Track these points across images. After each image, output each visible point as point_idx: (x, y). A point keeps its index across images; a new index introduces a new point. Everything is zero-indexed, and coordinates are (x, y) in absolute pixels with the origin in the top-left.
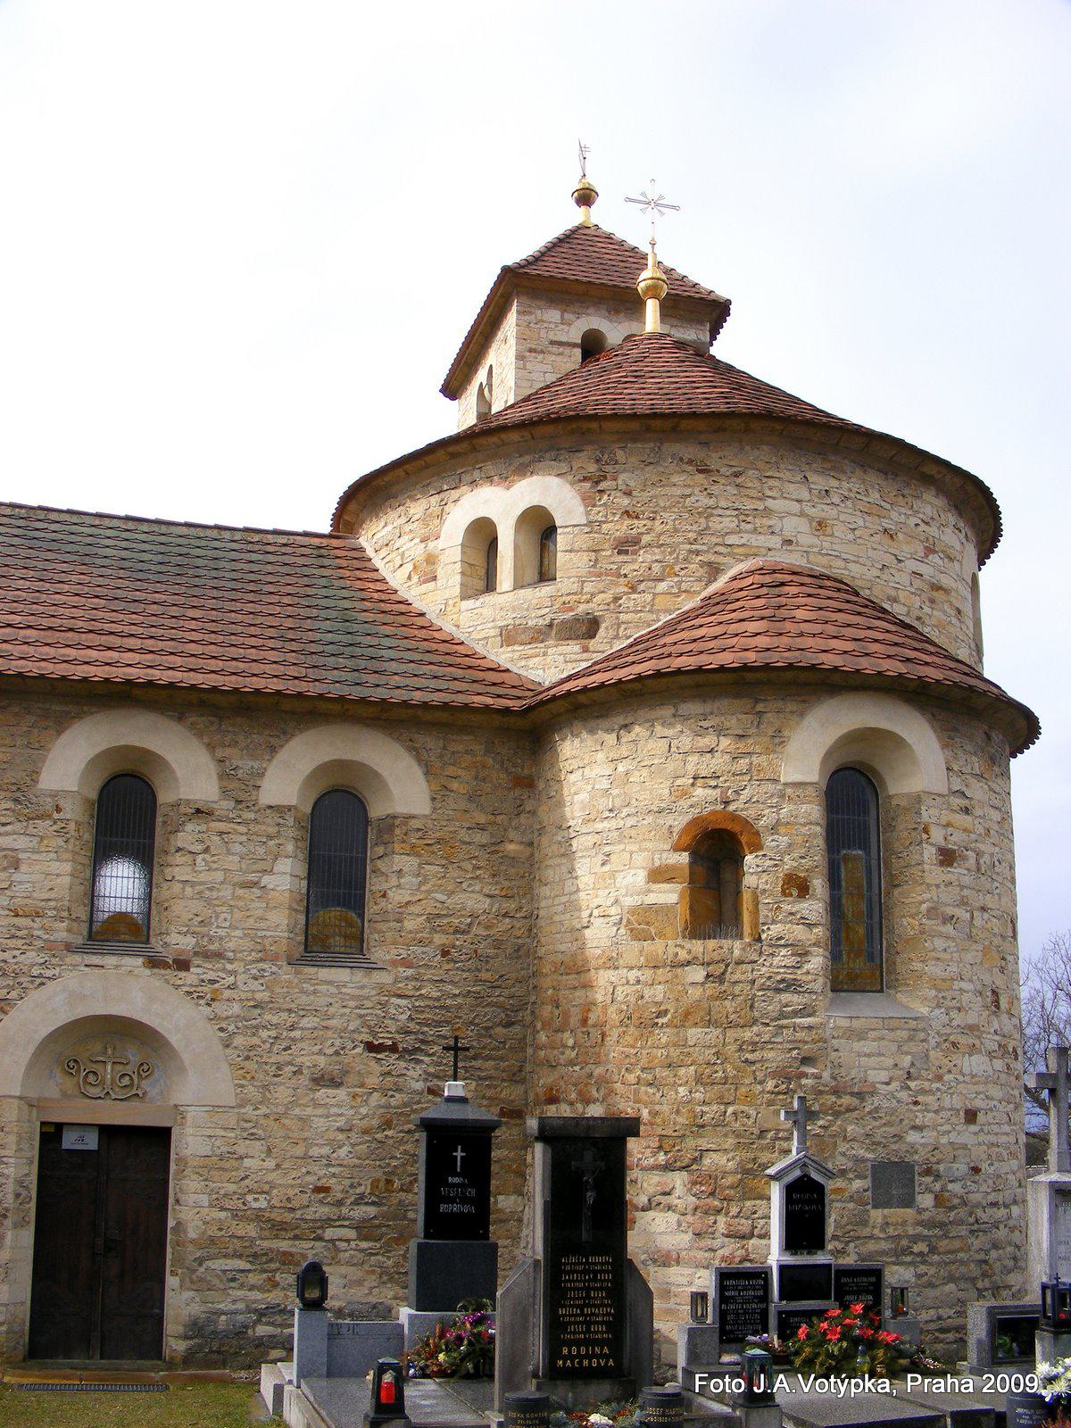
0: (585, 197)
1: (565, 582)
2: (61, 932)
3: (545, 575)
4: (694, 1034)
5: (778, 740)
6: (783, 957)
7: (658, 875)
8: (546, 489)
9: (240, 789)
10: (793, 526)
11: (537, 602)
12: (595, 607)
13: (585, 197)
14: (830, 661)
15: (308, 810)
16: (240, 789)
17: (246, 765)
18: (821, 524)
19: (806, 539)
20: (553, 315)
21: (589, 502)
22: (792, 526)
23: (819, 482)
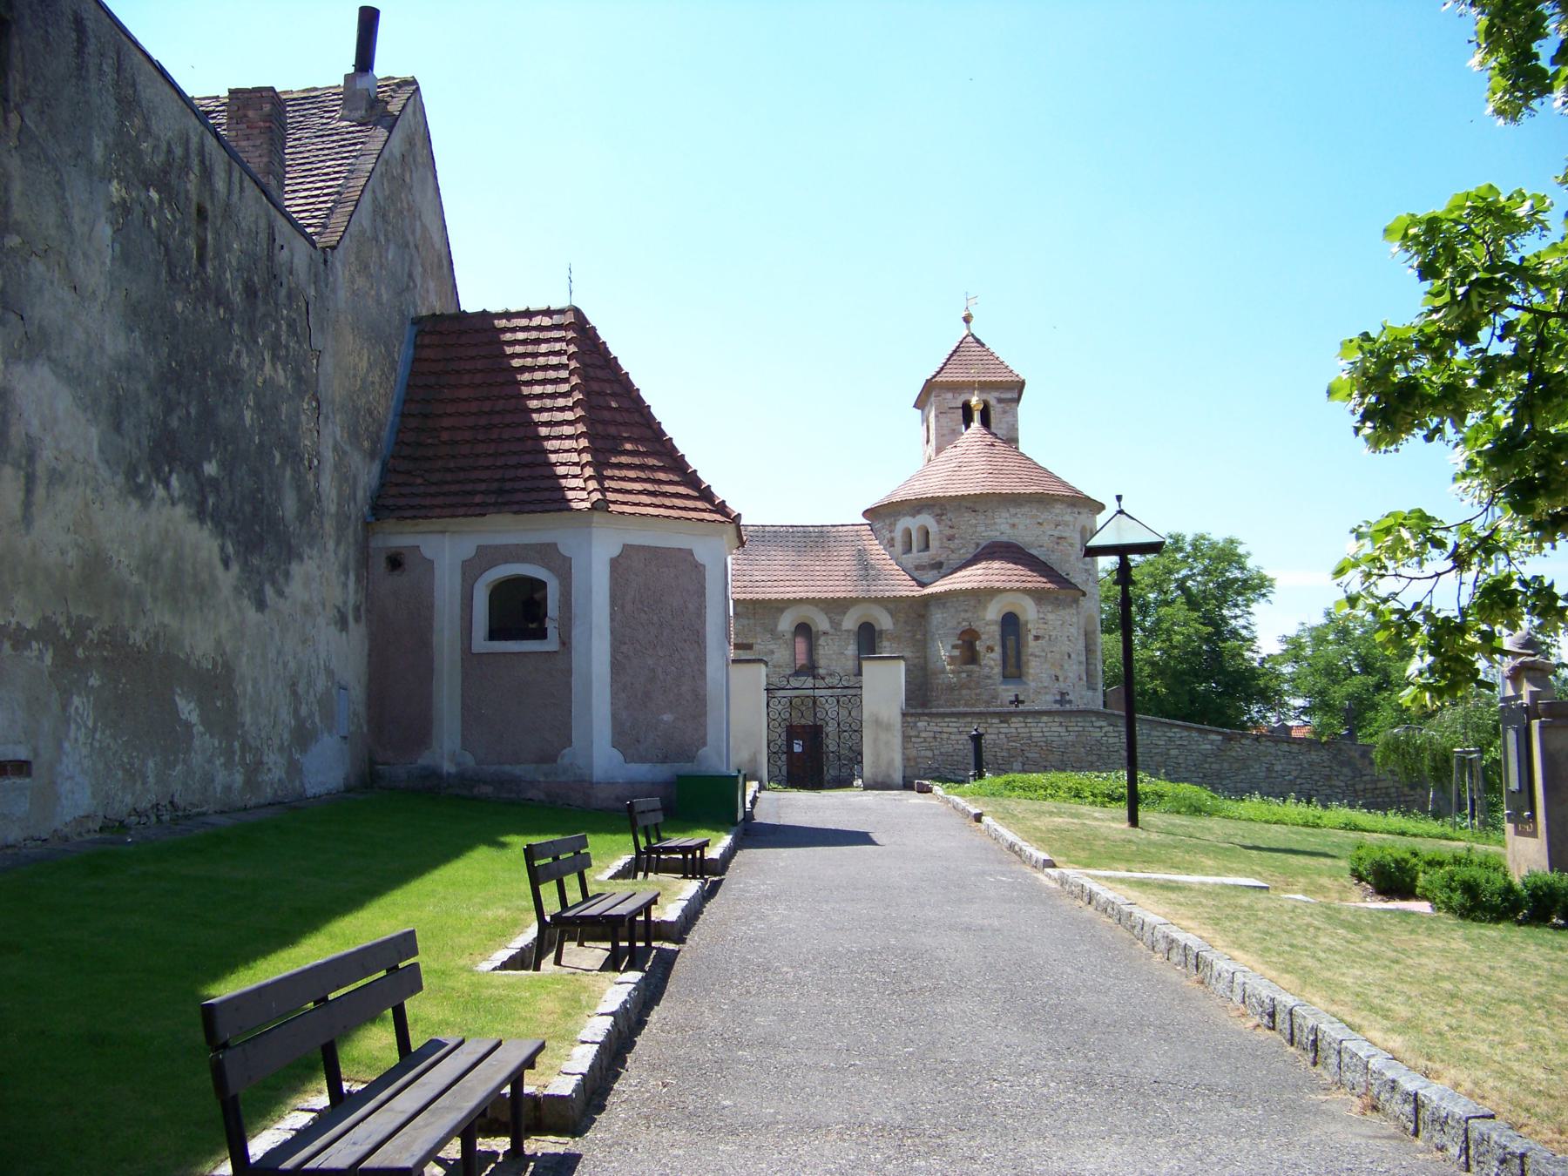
0: (967, 319)
1: (933, 551)
2: (788, 672)
3: (927, 547)
4: (964, 692)
5: (985, 608)
6: (987, 670)
7: (954, 647)
8: (926, 520)
9: (836, 625)
10: (1005, 527)
11: (925, 557)
12: (942, 558)
13: (967, 319)
14: (997, 585)
15: (856, 628)
16: (836, 625)
17: (838, 618)
18: (1014, 525)
19: (1009, 531)
20: (949, 395)
21: (938, 522)
22: (1005, 527)
23: (1013, 511)
